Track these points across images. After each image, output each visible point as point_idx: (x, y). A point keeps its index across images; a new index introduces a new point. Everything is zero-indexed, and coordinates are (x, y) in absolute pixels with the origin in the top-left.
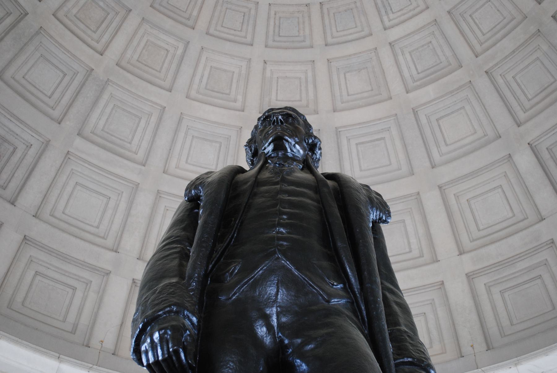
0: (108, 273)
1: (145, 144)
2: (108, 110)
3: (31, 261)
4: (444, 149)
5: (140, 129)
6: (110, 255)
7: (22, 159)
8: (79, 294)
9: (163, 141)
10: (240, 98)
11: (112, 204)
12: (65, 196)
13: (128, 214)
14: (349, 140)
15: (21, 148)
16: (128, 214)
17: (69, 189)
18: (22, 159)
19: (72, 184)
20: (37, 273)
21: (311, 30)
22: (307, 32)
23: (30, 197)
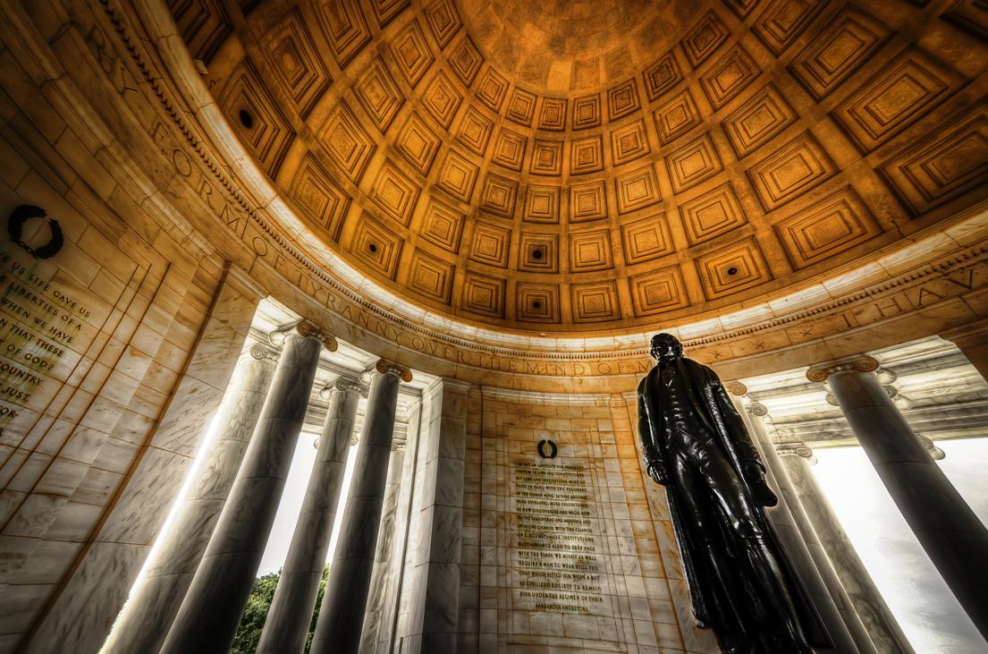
0: (615, 280)
1: (603, 206)
2: (577, 200)
3: (578, 292)
4: (828, 79)
5: (597, 199)
6: (611, 272)
7: (552, 249)
8: (606, 296)
9: (612, 199)
10: (645, 145)
11: (600, 245)
12: (578, 254)
13: (611, 247)
14: (733, 124)
15: (548, 245)
16: (611, 247)
17: (578, 250)
18: (552, 249)
19: (578, 246)
20: (583, 296)
21: (679, 67)
22: (676, 69)
23: (564, 265)
